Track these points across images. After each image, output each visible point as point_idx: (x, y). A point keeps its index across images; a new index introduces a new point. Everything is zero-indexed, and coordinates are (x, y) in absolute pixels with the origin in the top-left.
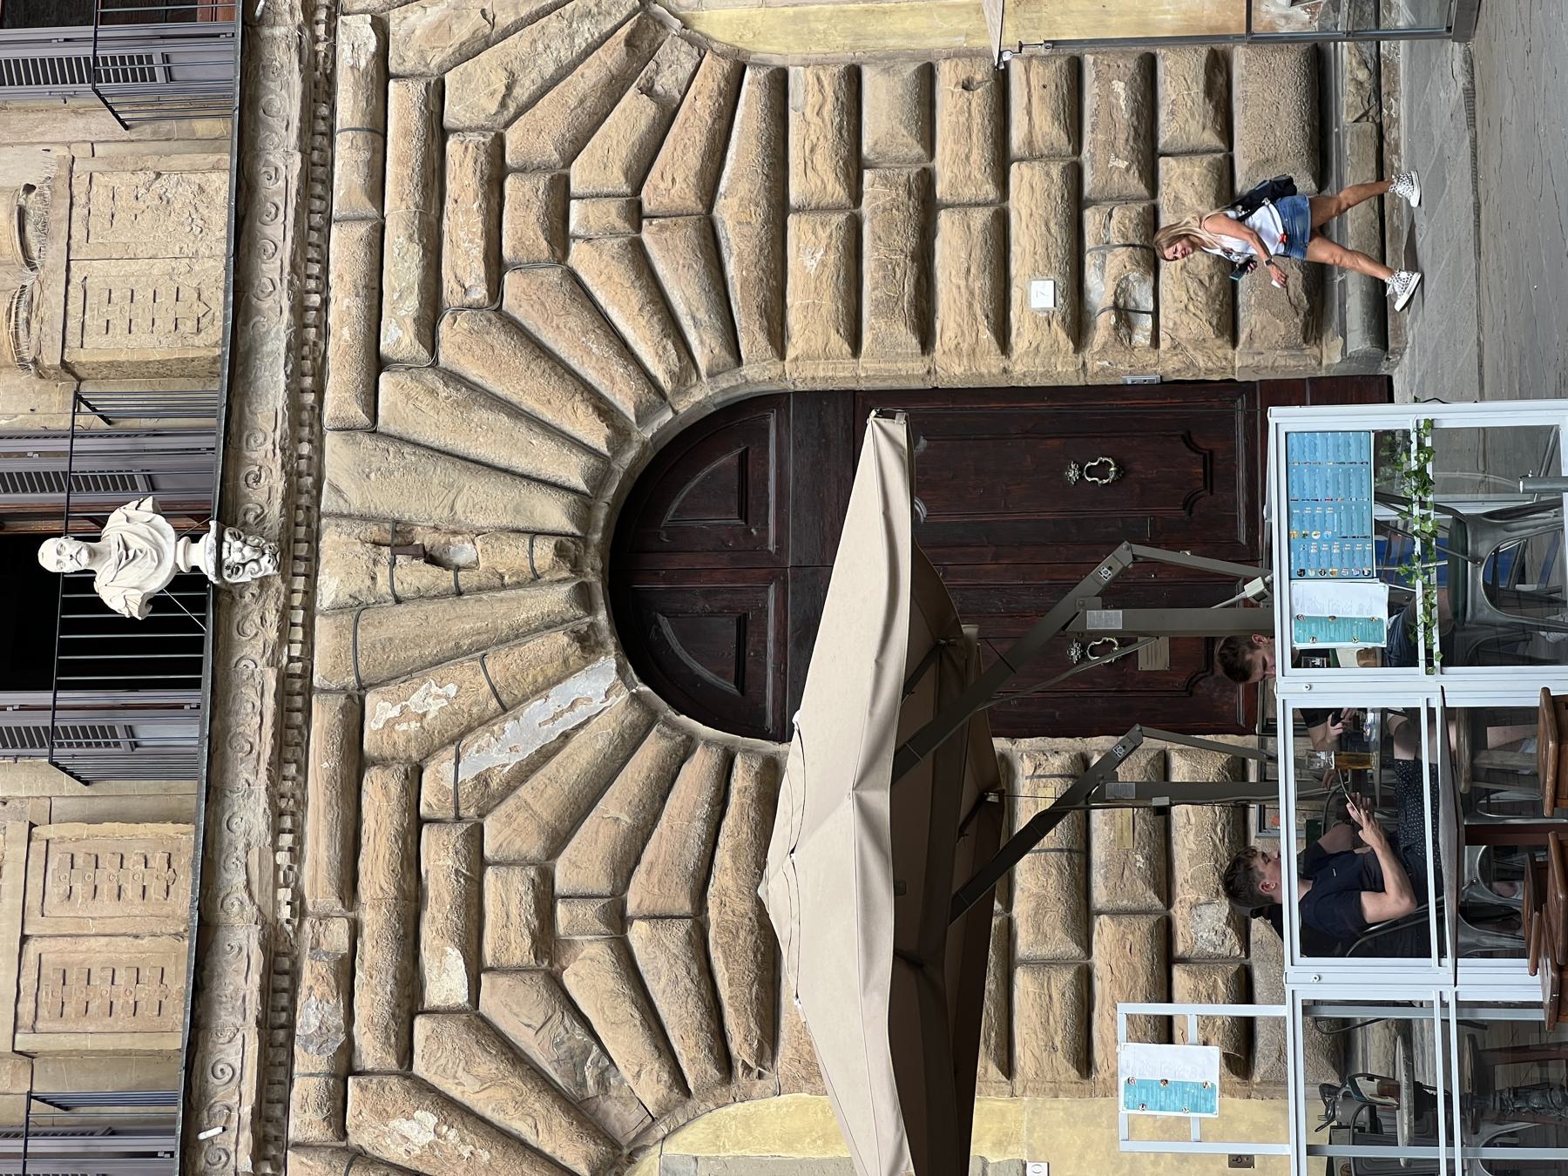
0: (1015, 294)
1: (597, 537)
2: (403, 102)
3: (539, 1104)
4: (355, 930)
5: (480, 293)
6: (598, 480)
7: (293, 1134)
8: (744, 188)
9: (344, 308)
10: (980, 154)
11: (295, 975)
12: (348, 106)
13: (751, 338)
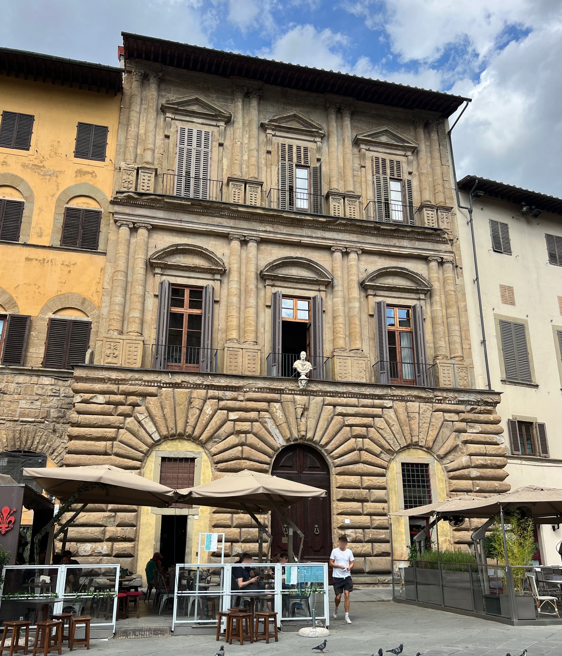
0: (347, 516)
2: (378, 411)
3: (212, 431)
4: (242, 401)
5: (346, 423)
6: (315, 442)
7: (209, 391)
8: (365, 469)
9: (344, 400)
10: (371, 511)
11: (235, 391)
12: (377, 402)
13: (339, 469)
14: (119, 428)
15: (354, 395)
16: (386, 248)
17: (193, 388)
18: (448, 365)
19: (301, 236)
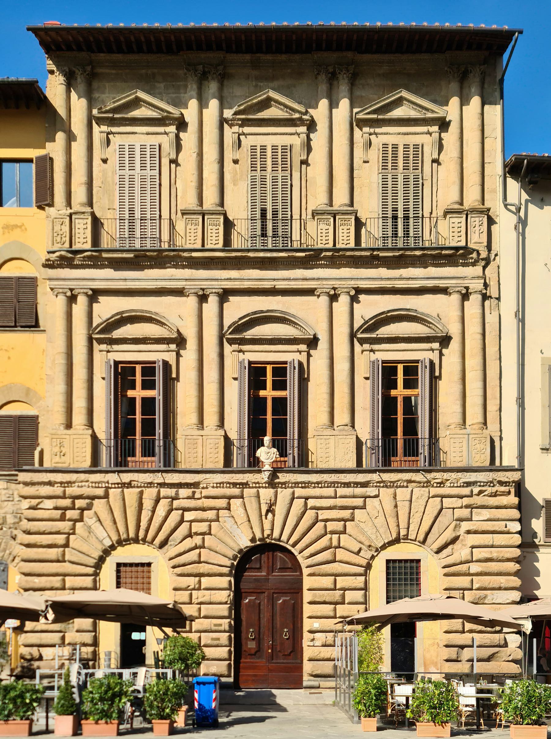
1: (273, 541)
3: (168, 532)
9: (317, 492)
12: (359, 491)
13: (310, 570)
14: (69, 534)
15: (332, 484)
16: (389, 282)
17: (144, 487)
18: (461, 436)
19: (274, 280)
